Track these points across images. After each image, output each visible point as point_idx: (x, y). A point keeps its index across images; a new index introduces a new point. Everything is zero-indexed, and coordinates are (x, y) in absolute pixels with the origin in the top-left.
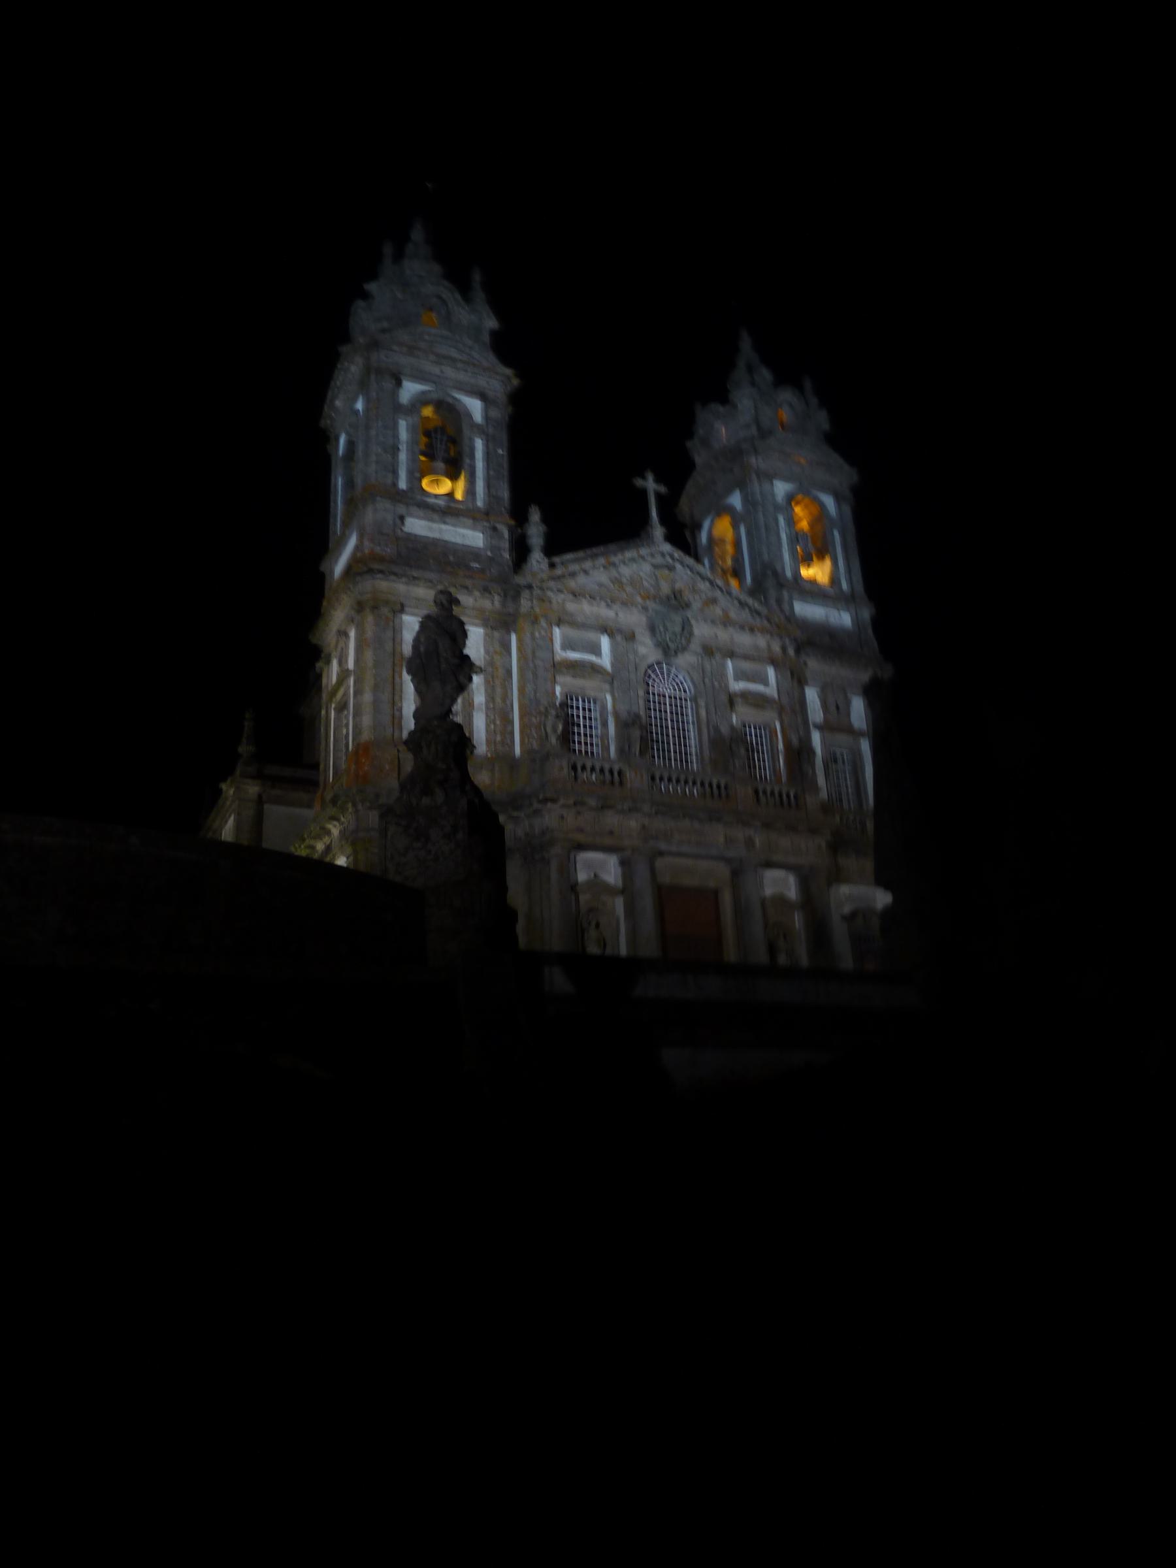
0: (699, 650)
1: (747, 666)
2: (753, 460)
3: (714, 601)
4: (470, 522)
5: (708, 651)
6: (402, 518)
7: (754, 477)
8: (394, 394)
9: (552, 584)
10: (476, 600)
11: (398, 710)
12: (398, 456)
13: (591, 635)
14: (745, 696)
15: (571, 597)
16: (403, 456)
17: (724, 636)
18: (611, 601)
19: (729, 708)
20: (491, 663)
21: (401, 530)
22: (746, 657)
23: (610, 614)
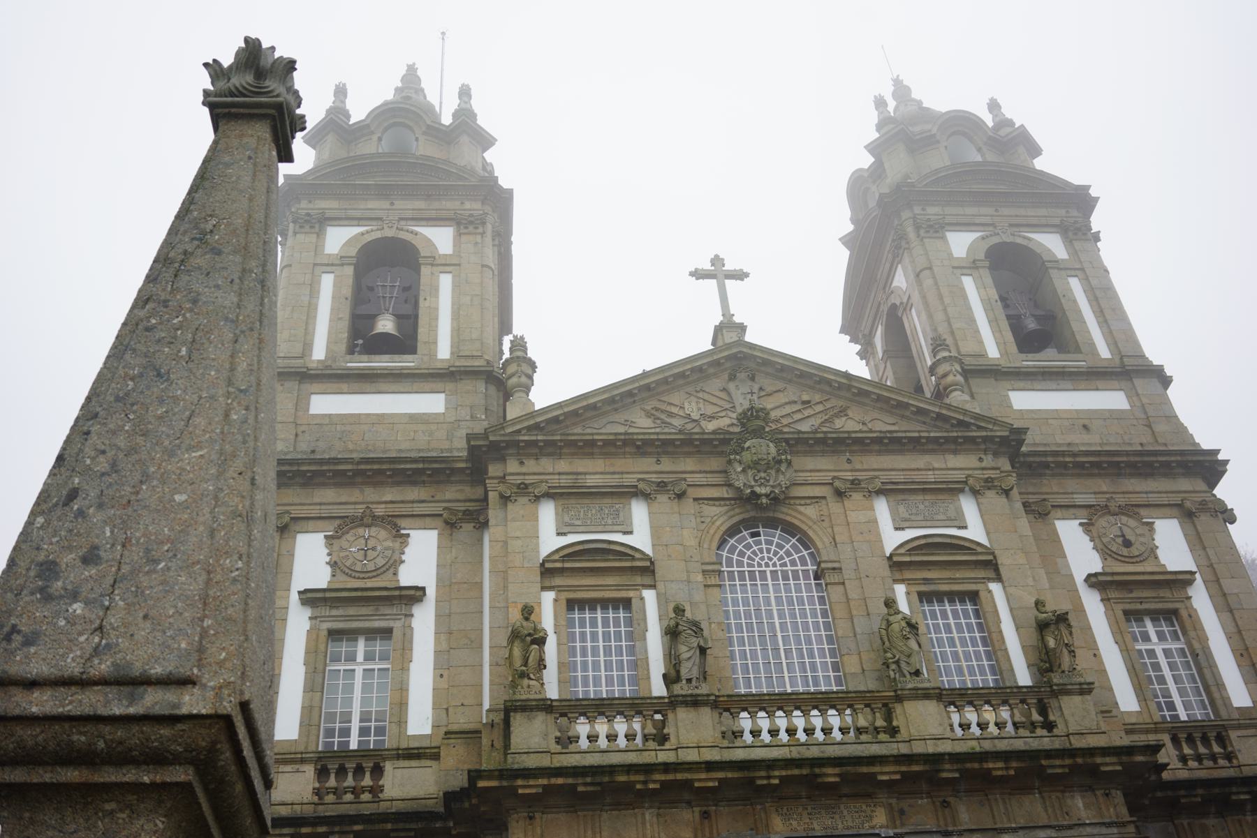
3: (842, 412)
8: (318, 247)
23: (647, 464)
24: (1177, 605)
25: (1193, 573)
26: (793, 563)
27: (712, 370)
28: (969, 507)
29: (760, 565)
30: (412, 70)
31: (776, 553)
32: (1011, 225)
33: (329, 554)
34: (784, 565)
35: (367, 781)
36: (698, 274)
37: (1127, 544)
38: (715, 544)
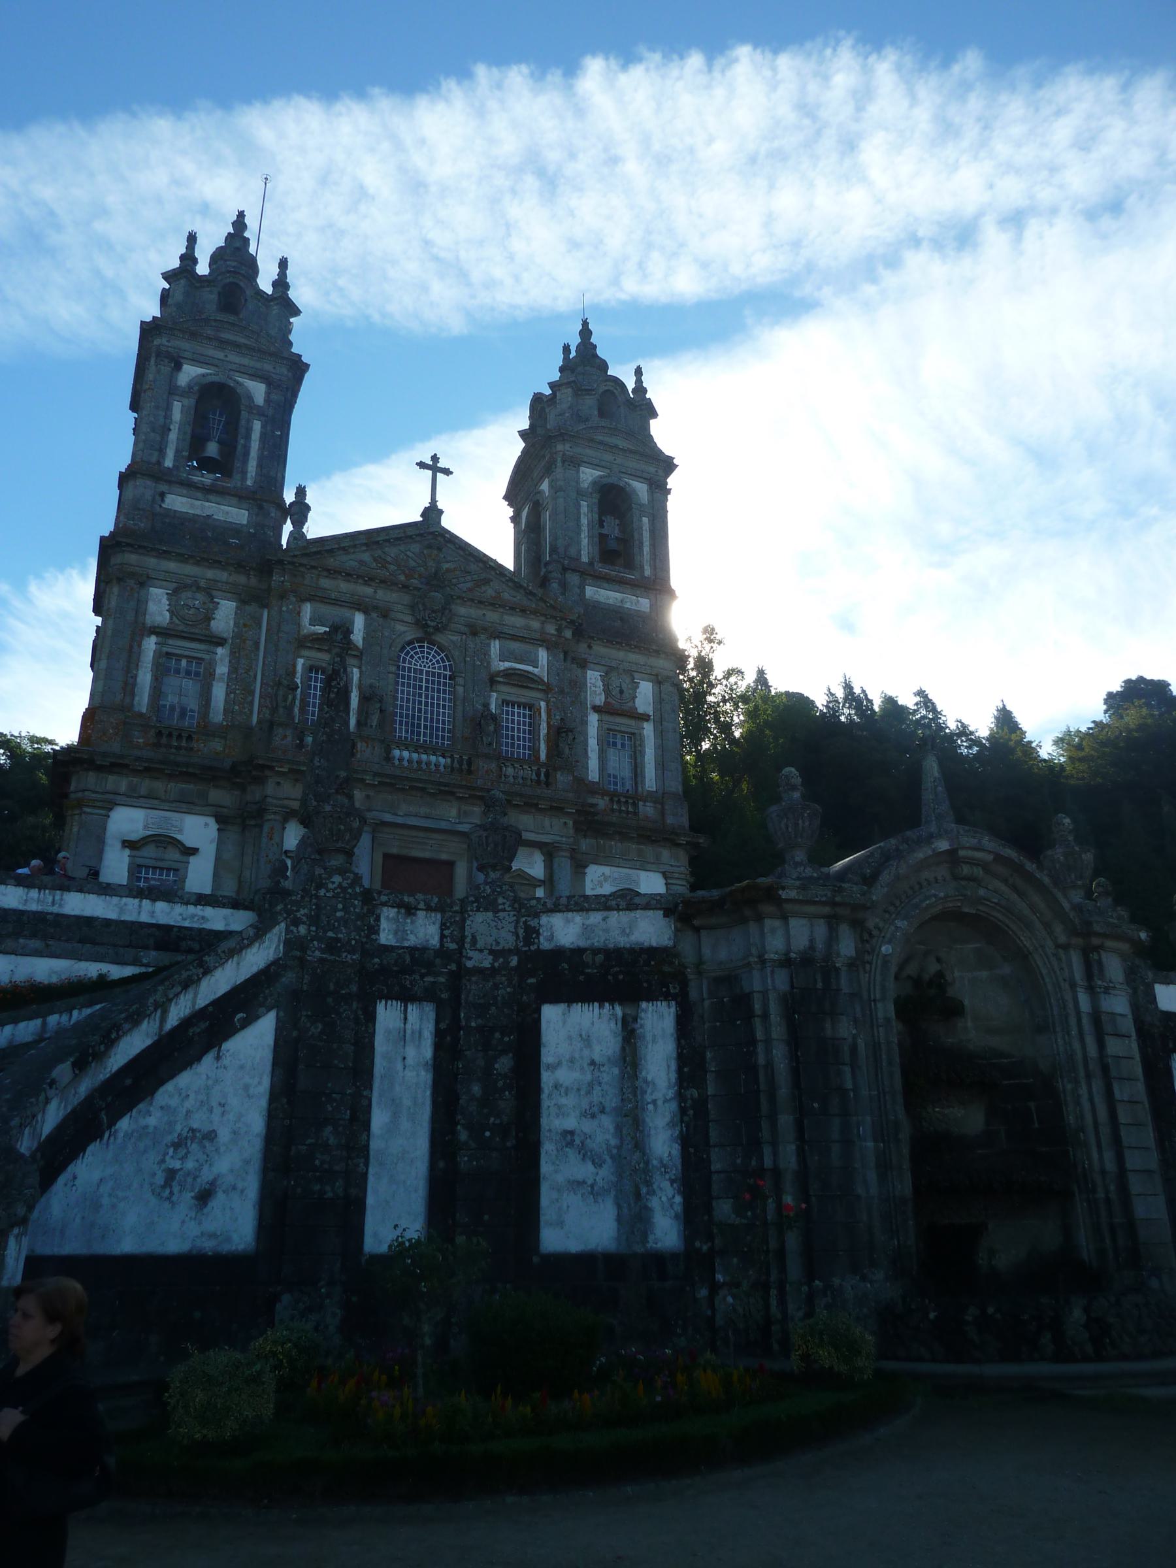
0: (464, 629)
1: (515, 646)
2: (560, 447)
4: (234, 500)
5: (474, 631)
6: (162, 495)
7: (559, 464)
9: (305, 561)
10: (230, 575)
11: (132, 677)
12: (168, 435)
13: (344, 612)
14: (509, 674)
15: (325, 573)
16: (173, 436)
17: (492, 616)
18: (369, 580)
19: (488, 684)
20: (238, 635)
21: (161, 506)
22: (514, 638)
23: (369, 591)
24: (636, 731)
25: (649, 716)
26: (439, 668)
27: (418, 538)
28: (543, 655)
29: (421, 666)
30: (241, 215)
31: (431, 660)
32: (620, 472)
33: (169, 605)
34: (434, 668)
35: (184, 744)
36: (422, 465)
37: (621, 692)
38: (399, 647)
